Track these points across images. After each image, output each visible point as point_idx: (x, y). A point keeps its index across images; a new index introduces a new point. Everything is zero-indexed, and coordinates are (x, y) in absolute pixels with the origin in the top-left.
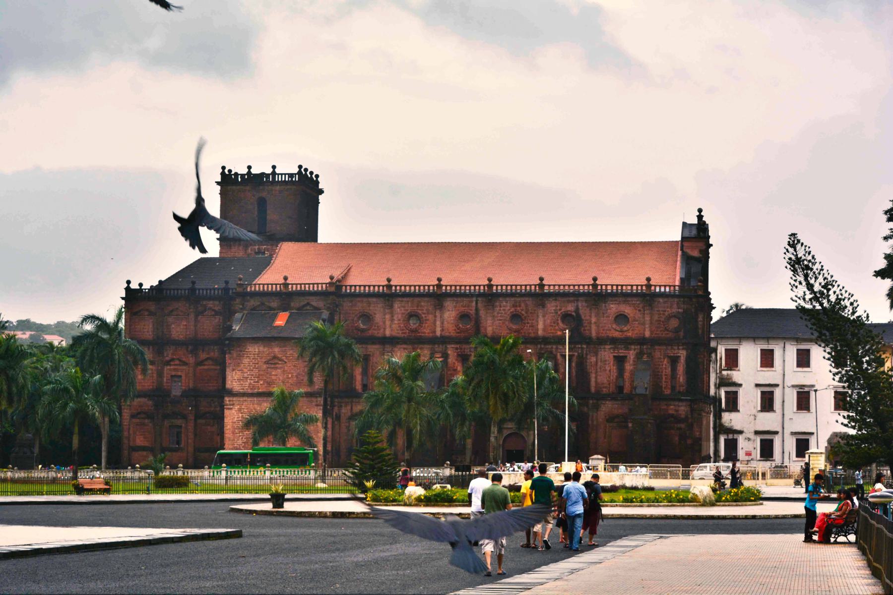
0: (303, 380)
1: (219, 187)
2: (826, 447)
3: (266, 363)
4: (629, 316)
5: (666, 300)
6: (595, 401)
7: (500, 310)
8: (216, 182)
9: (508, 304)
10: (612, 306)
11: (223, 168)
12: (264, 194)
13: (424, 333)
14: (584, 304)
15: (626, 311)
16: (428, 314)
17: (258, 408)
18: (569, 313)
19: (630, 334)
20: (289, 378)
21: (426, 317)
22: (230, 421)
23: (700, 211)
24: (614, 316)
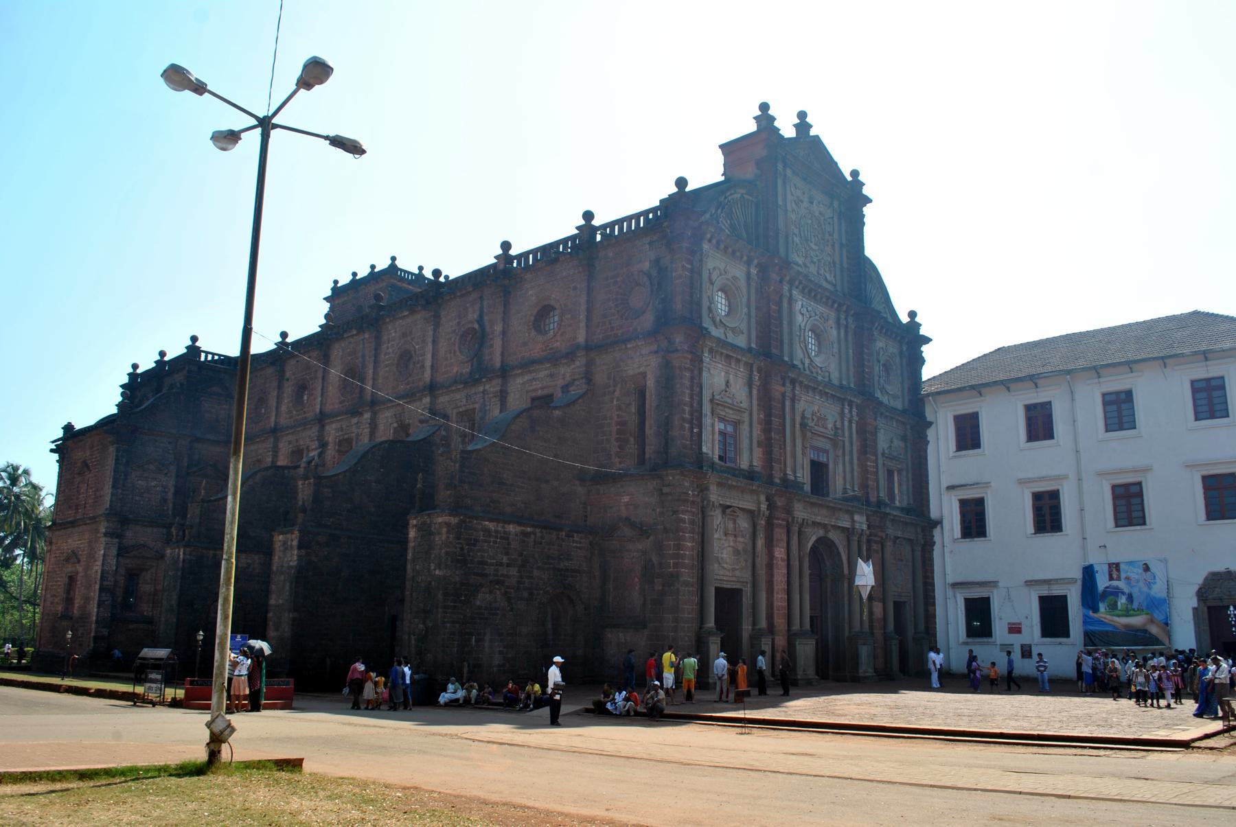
2: (1195, 609)
7: (388, 348)
8: (324, 299)
10: (531, 292)
18: (470, 326)
21: (312, 384)
24: (535, 312)
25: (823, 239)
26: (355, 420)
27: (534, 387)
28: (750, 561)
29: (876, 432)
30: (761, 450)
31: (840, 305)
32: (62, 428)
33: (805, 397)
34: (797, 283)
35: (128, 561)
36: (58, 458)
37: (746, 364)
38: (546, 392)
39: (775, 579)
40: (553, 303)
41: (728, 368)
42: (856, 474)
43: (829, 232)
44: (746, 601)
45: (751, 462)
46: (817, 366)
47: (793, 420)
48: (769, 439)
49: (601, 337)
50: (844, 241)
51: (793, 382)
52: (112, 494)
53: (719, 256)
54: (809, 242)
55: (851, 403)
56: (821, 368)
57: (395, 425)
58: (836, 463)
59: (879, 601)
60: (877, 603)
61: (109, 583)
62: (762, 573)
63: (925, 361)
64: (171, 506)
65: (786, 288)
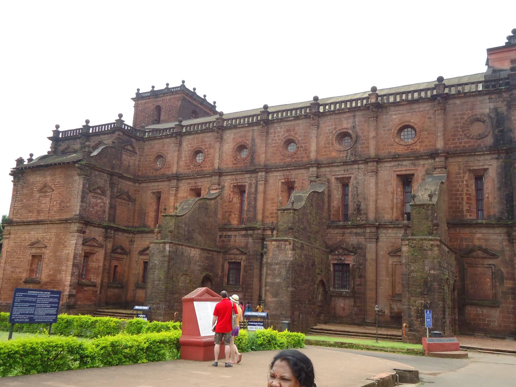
0: (63, 207)
1: (134, 103)
3: (40, 191)
4: (415, 127)
5: (463, 100)
6: (374, 230)
7: (274, 137)
8: (132, 99)
9: (283, 130)
10: (394, 117)
11: (138, 90)
12: (160, 103)
13: (206, 167)
14: (362, 119)
15: (412, 121)
16: (210, 148)
17: (28, 237)
18: (345, 130)
19: (418, 147)
20: (54, 206)
21: (208, 151)
22: (6, 250)
24: (398, 128)
26: (248, 176)
27: (400, 169)
32: (16, 160)
35: (85, 248)
36: (13, 179)
38: (408, 172)
40: (411, 124)
49: (452, 146)
52: (81, 206)
57: (283, 181)
61: (78, 261)
64: (107, 215)
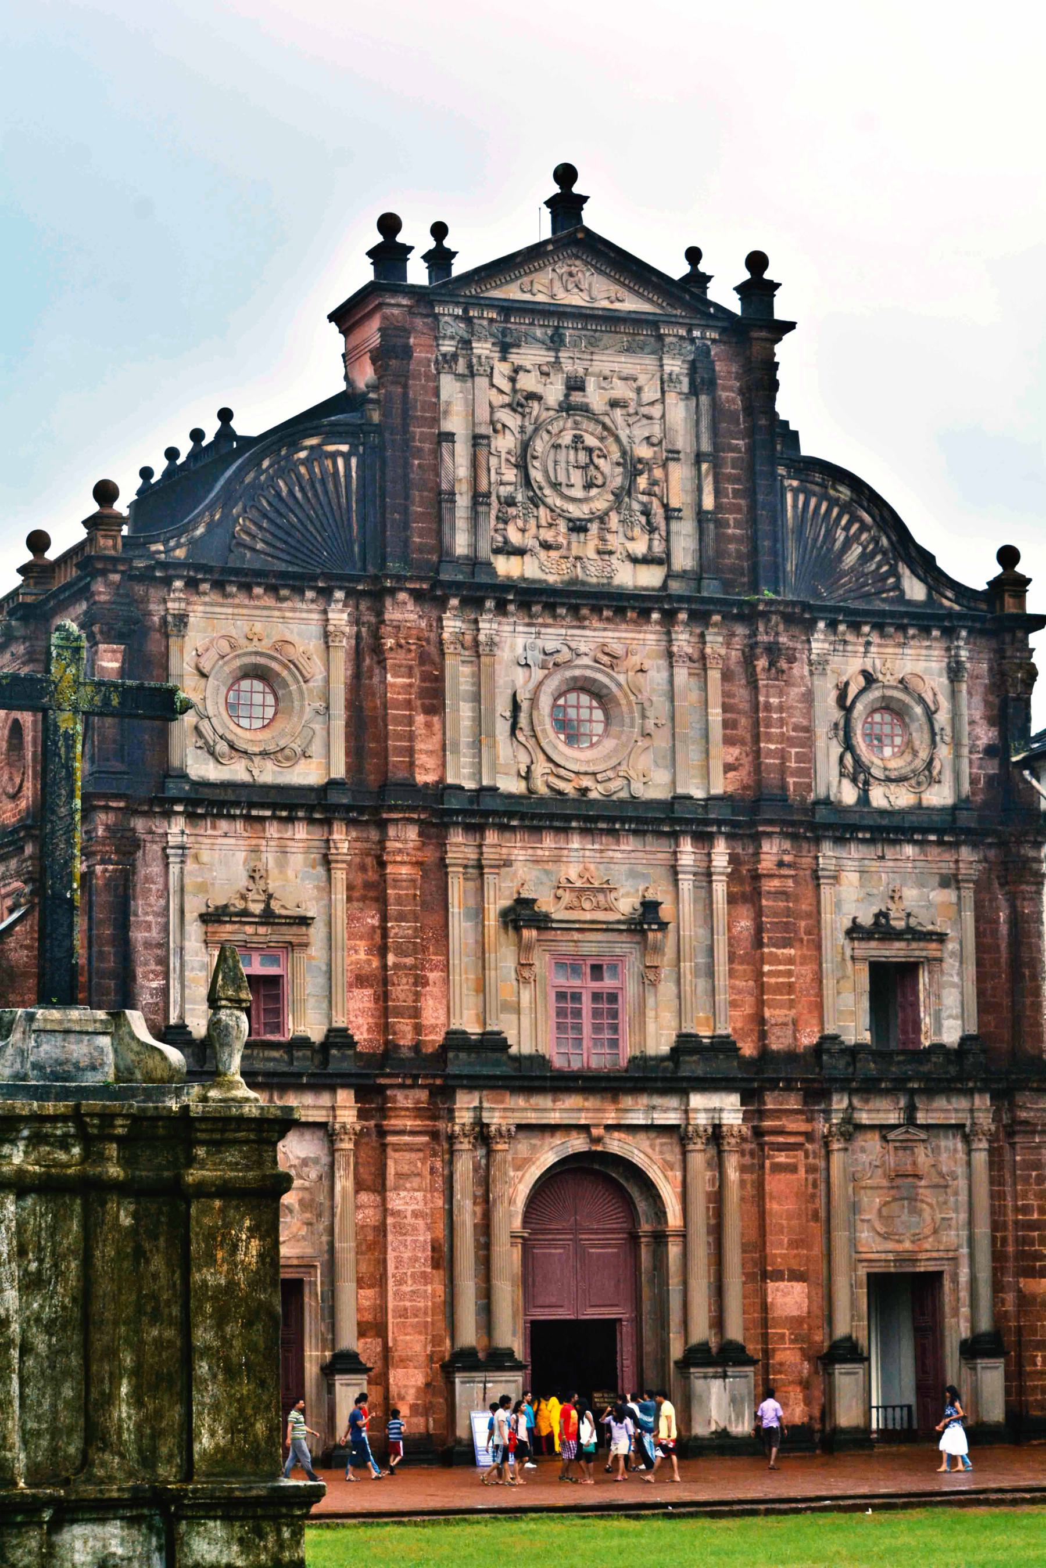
23: (566, 174)
24: (6, 732)
25: (618, 464)
28: (325, 1221)
29: (818, 885)
30: (368, 992)
31: (669, 617)
33: (530, 852)
34: (490, 604)
37: (311, 821)
39: (391, 1255)
41: (254, 842)
42: (722, 998)
43: (648, 438)
44: (311, 1304)
45: (330, 1023)
46: (577, 773)
47: (479, 913)
48: (384, 967)
50: (706, 446)
51: (476, 829)
53: (230, 611)
54: (565, 490)
55: (703, 839)
56: (594, 774)
58: (649, 978)
59: (797, 1276)
60: (782, 1285)
62: (346, 1247)
63: (1032, 674)
65: (452, 625)
